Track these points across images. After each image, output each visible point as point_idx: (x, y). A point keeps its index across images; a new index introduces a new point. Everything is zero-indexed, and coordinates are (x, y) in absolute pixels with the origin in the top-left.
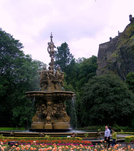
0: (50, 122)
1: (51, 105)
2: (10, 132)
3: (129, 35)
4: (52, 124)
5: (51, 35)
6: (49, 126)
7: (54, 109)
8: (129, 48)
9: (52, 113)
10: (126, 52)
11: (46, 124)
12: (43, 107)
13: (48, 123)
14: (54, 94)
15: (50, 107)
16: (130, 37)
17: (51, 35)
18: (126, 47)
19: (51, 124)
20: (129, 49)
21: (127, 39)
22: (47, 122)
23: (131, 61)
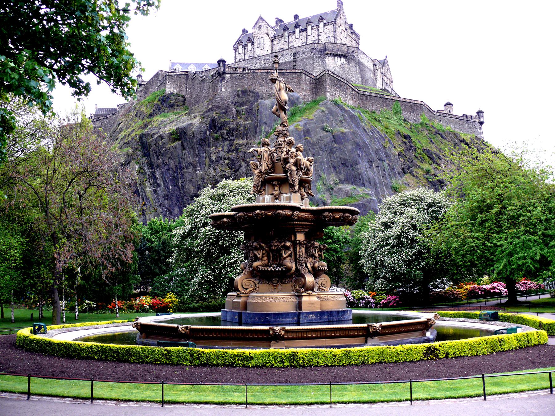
0: (313, 290)
1: (304, 244)
2: (175, 325)
3: (149, 111)
7: (313, 256)
8: (161, 137)
9: (309, 265)
10: (155, 144)
11: (305, 299)
12: (287, 248)
13: (310, 295)
14: (326, 213)
16: (151, 115)
18: (154, 134)
20: (162, 139)
21: (143, 119)
22: (305, 292)
23: (166, 163)
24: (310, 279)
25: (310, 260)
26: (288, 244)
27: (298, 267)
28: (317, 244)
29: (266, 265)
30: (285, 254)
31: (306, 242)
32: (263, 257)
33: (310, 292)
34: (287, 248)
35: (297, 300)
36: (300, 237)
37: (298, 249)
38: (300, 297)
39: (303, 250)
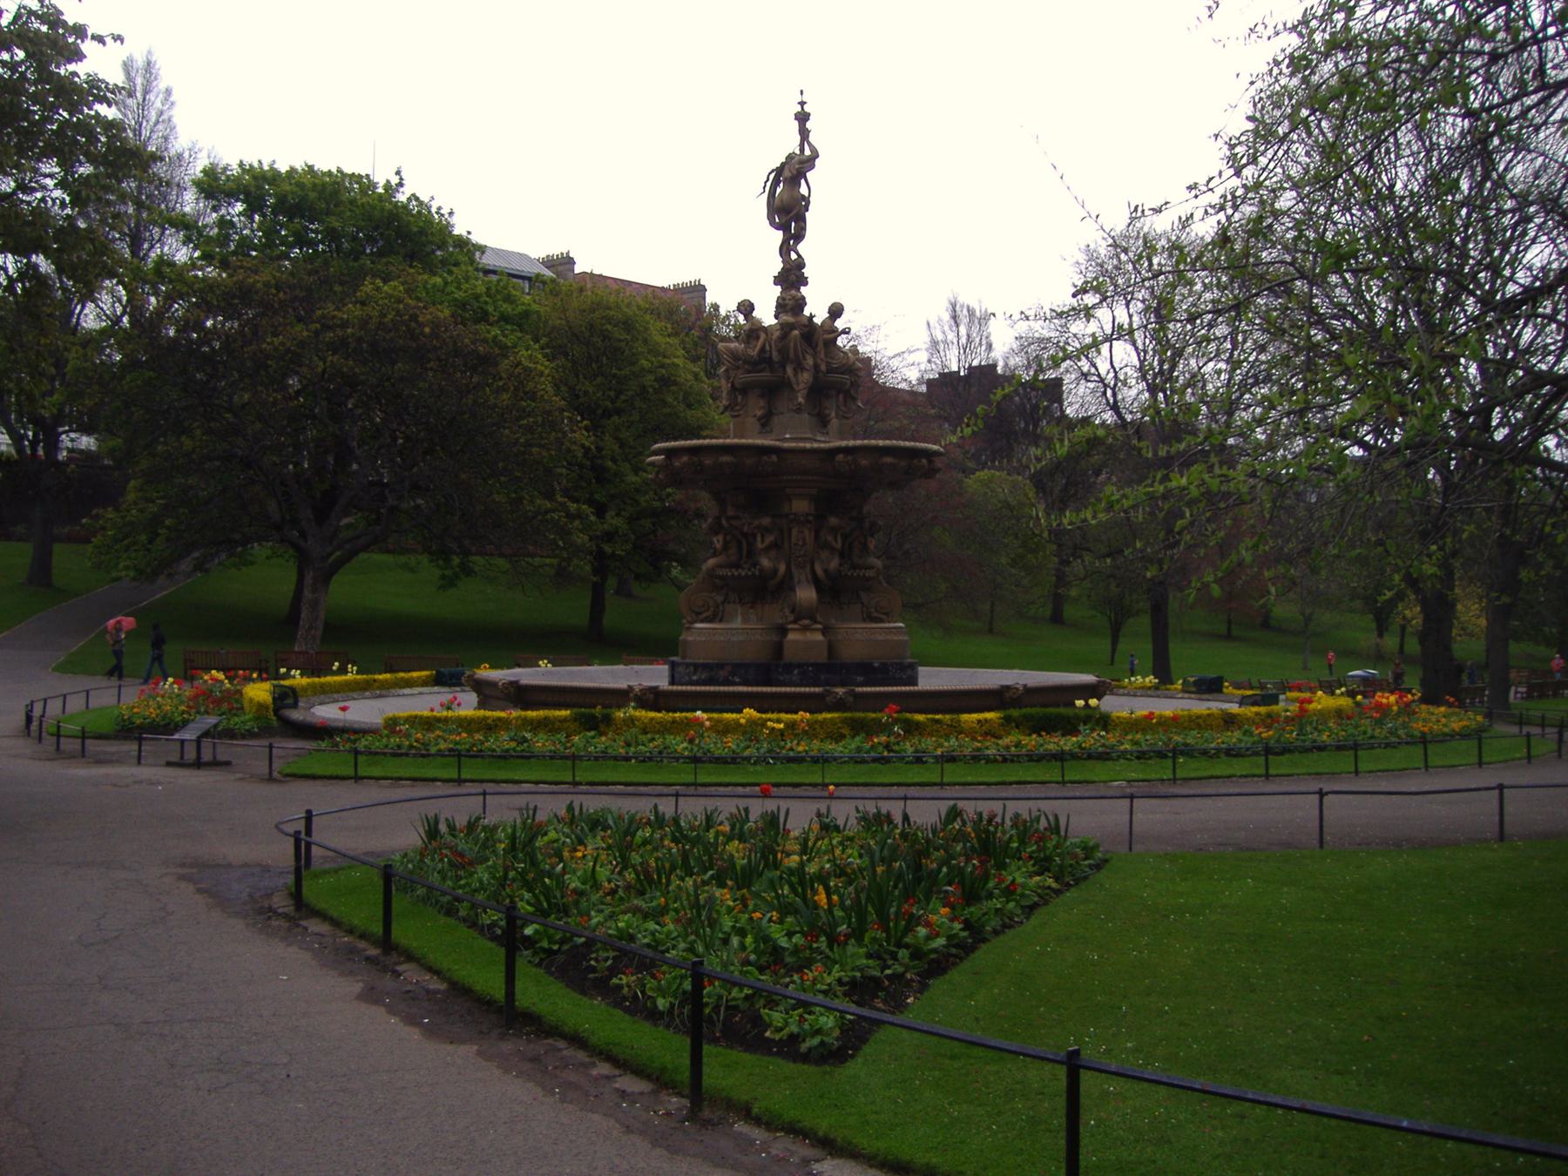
1: (810, 522)
4: (824, 632)
5: (802, 104)
6: (804, 641)
11: (791, 636)
13: (805, 629)
14: (840, 457)
15: (807, 532)
17: (802, 104)
19: (819, 637)
22: (794, 622)
24: (806, 594)
25: (825, 554)
26: (766, 521)
27: (793, 568)
28: (833, 521)
29: (738, 566)
30: (763, 541)
31: (811, 518)
32: (726, 546)
33: (806, 622)
34: (766, 530)
35: (775, 638)
36: (801, 506)
37: (794, 532)
38: (783, 631)
39: (809, 535)
